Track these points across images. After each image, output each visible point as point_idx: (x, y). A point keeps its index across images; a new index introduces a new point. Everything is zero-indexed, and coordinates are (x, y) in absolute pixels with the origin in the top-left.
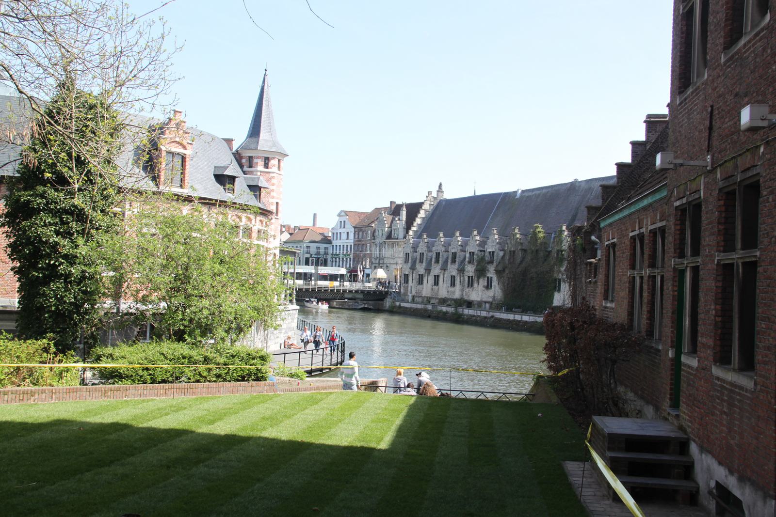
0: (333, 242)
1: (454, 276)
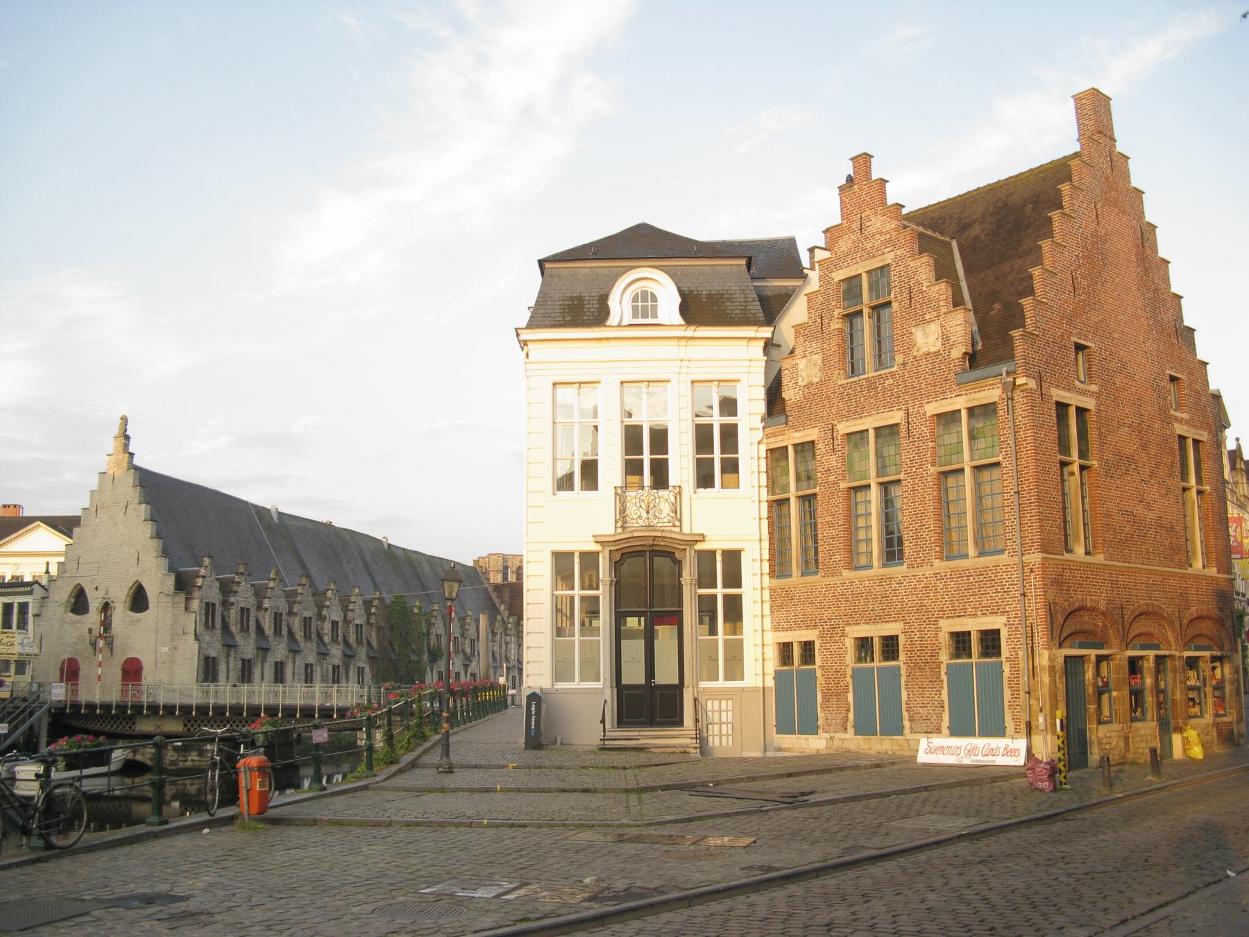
1: (312, 665)
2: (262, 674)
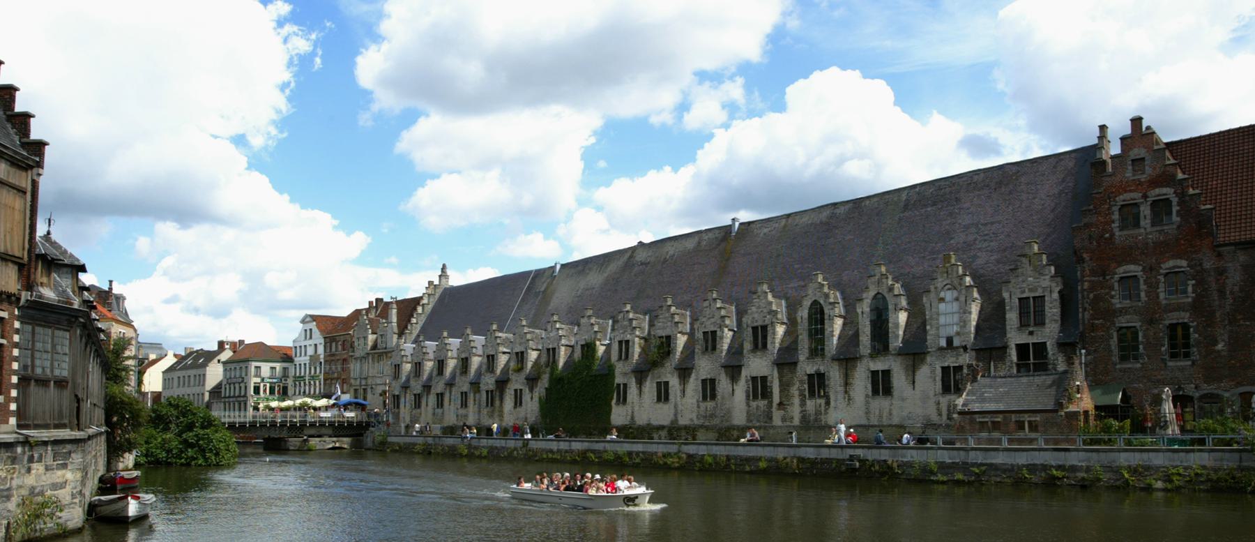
0: (296, 359)
2: (450, 399)
